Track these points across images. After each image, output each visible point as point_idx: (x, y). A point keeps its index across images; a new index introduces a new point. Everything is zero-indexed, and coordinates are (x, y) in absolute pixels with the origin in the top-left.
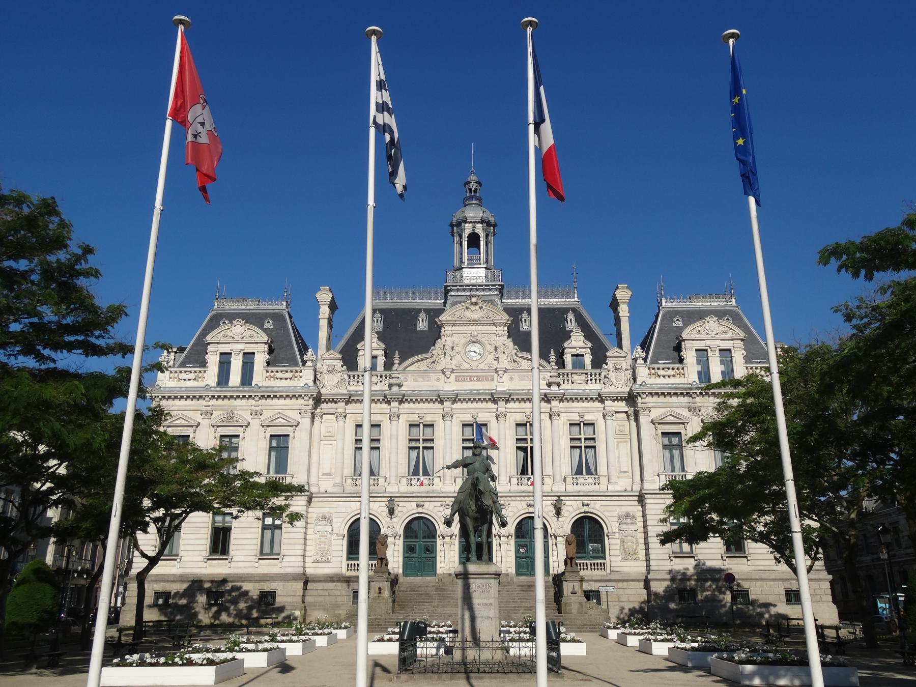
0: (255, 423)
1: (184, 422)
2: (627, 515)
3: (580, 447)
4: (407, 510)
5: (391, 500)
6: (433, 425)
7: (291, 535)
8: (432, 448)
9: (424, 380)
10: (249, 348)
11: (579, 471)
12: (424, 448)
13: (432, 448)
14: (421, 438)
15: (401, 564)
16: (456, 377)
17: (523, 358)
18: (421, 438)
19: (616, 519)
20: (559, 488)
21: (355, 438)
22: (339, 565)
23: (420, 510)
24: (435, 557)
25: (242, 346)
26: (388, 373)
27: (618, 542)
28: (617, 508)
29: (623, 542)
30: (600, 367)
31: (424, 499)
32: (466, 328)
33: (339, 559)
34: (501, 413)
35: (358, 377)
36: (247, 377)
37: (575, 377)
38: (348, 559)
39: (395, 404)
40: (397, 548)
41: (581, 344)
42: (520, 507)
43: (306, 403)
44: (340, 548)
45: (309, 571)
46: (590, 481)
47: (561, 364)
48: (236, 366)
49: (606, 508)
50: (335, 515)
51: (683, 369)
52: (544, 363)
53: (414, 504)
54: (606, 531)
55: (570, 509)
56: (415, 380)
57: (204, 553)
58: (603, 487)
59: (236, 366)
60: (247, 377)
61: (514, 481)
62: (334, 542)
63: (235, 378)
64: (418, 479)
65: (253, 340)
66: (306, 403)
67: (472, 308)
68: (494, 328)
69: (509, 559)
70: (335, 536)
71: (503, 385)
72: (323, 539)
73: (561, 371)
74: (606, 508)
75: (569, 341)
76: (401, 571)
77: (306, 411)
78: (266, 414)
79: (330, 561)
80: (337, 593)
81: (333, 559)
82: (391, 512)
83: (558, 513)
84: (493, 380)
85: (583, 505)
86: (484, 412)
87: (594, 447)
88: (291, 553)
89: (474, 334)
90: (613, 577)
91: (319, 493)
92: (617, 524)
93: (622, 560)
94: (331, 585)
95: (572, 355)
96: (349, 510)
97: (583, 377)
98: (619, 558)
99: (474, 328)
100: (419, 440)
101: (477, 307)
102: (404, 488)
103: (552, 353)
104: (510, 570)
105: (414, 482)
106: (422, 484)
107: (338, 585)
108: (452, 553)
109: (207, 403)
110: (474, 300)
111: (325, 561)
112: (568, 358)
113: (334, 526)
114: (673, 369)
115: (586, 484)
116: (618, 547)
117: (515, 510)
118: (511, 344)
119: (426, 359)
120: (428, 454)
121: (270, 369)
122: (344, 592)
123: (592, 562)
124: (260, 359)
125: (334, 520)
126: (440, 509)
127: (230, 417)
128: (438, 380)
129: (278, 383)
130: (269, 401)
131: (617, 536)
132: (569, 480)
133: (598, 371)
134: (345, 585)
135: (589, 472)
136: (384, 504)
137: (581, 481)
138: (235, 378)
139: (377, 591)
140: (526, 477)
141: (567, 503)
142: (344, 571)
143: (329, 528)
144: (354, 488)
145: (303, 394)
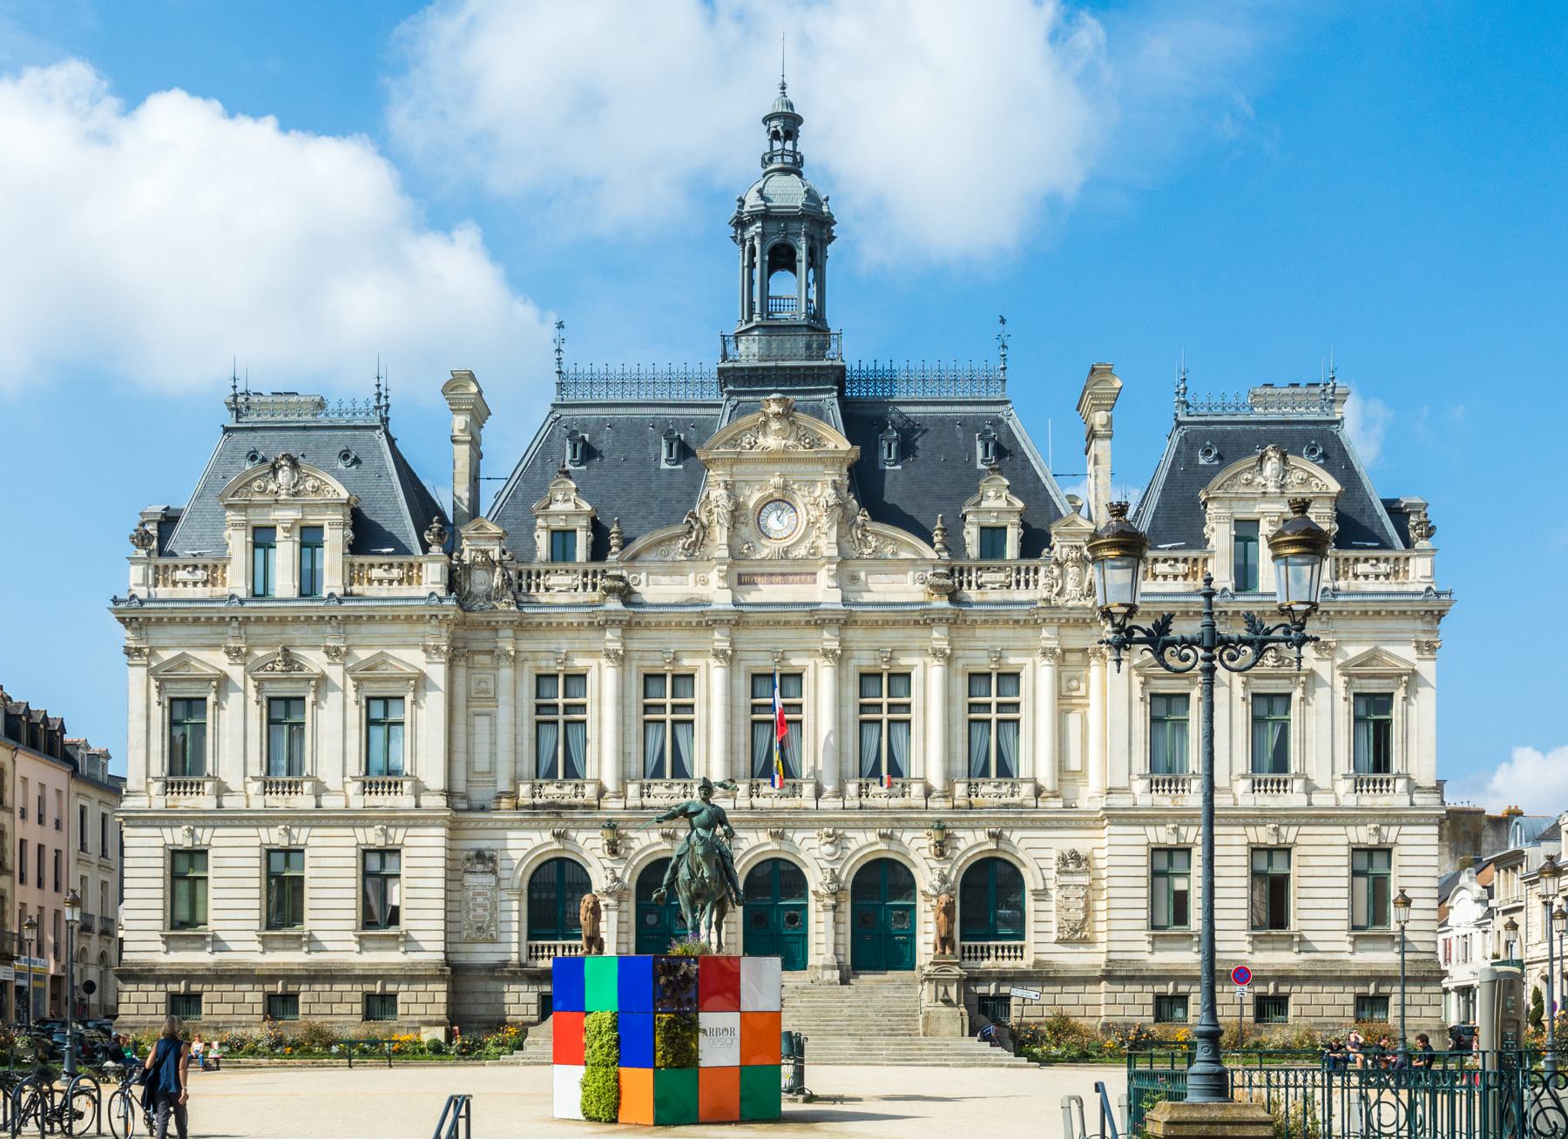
2: (1076, 857)
10: (313, 519)
16: (740, 575)
18: (668, 701)
21: (534, 701)
27: (1053, 906)
30: (1038, 555)
35: (538, 576)
38: (531, 937)
40: (624, 917)
49: (1031, 843)
51: (1206, 560)
57: (256, 925)
72: (480, 900)
74: (1031, 843)
77: (437, 648)
91: (470, 810)
93: (1059, 941)
95: (983, 529)
98: (1054, 937)
111: (486, 941)
112: (971, 536)
114: (1185, 560)
116: (1053, 916)
119: (678, 537)
121: (359, 560)
123: (1000, 943)
124: (334, 540)
128: (705, 583)
130: (365, 629)
143: (489, 880)
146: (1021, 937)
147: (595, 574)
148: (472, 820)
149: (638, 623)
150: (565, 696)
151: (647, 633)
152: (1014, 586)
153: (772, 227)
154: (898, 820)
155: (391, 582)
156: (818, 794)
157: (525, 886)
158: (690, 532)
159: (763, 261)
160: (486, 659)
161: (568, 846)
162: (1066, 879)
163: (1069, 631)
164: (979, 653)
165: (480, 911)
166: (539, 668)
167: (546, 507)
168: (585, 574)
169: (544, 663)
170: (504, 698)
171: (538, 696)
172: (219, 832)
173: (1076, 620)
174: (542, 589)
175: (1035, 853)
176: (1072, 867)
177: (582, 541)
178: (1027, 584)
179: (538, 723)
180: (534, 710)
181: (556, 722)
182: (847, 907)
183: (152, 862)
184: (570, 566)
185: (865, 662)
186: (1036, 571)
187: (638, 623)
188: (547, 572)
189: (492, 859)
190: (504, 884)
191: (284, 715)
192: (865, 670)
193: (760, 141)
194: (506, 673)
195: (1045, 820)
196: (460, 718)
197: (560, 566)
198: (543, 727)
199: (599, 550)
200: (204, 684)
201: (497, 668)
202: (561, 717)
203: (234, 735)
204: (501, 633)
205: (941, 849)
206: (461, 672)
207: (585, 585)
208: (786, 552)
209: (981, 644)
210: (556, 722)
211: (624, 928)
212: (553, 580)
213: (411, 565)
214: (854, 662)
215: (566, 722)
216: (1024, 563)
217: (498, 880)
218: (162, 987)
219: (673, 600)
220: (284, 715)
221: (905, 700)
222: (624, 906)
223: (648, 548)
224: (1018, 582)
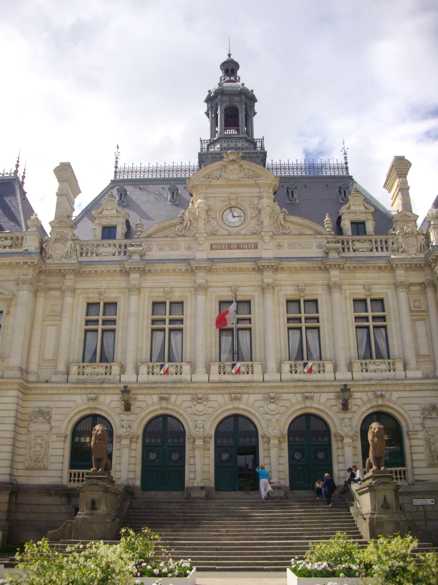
3: (368, 327)
4: (148, 406)
5: (126, 391)
6: (182, 303)
8: (181, 330)
9: (172, 249)
11: (368, 355)
12: (171, 330)
13: (181, 330)
14: (167, 317)
15: (139, 473)
16: (211, 245)
17: (292, 223)
19: (418, 414)
20: (343, 375)
22: (59, 474)
23: (164, 404)
24: (184, 466)
26: (128, 242)
27: (421, 442)
28: (419, 400)
31: (169, 391)
32: (223, 190)
33: (59, 466)
34: (268, 285)
37: (358, 245)
38: (72, 466)
39: (134, 276)
41: (362, 208)
42: (294, 400)
44: (61, 452)
45: (22, 481)
46: (383, 367)
47: (339, 230)
49: (405, 401)
50: (54, 412)
52: (319, 228)
53: (156, 398)
54: (404, 429)
55: (359, 402)
56: (161, 249)
58: (400, 373)
61: (286, 367)
62: (52, 445)
64: (162, 366)
66: (25, 272)
67: (231, 167)
68: (257, 190)
69: (281, 468)
70: (54, 438)
71: (268, 251)
72: (39, 441)
73: (340, 237)
75: (347, 205)
76: (138, 483)
79: (46, 469)
81: (53, 466)
82: (127, 408)
83: (345, 407)
84: (256, 248)
85: (377, 397)
86: (246, 285)
87: (385, 327)
89: (232, 196)
90: (418, 488)
91: (38, 382)
92: (418, 421)
94: (48, 500)
95: (352, 223)
96: (72, 404)
97: (367, 245)
99: (233, 190)
100: (164, 321)
101: (236, 166)
102: (143, 377)
103: (327, 218)
104: (282, 482)
105: (157, 370)
106: (167, 372)
107: (57, 500)
108: (206, 461)
110: (231, 157)
111: (39, 469)
112: (346, 225)
113: (54, 423)
115: (377, 369)
116: (422, 449)
117: (288, 404)
118: (278, 208)
119: (175, 225)
120: (176, 338)
125: (54, 417)
126: (189, 404)
131: (421, 435)
132: (357, 366)
133: (384, 238)
134: (64, 500)
135: (379, 356)
136: (117, 397)
137: (372, 367)
139: (89, 505)
140: (302, 362)
141: (356, 395)
142: (65, 481)
143: (46, 427)
144: (81, 377)
146: (403, 464)
147: (126, 247)
148: (38, 388)
149: (150, 271)
150: (104, 314)
151: (155, 277)
152: (375, 250)
153: (226, 98)
154: (318, 387)
155: (5, 247)
156: (264, 371)
157: (69, 432)
158: (182, 223)
159: (221, 112)
160: (56, 293)
161: (99, 406)
162: (429, 423)
163: (410, 273)
164: (359, 287)
165: (38, 448)
166: (88, 298)
167: (101, 213)
168: (120, 247)
169: (91, 295)
170: (66, 315)
171: (87, 315)
173: (416, 265)
174: (94, 255)
175: (407, 407)
177: (121, 230)
178: (382, 250)
179: (86, 331)
180: (84, 323)
181: (96, 331)
182: (285, 446)
184: (111, 241)
185: (289, 293)
186: (386, 242)
187: (150, 271)
188: (98, 246)
189: (48, 413)
190: (55, 430)
192: (290, 298)
193: (220, 73)
194: (69, 300)
195: (411, 385)
196: (38, 326)
197: (106, 242)
198: (89, 334)
199: (128, 235)
201: (63, 298)
202: (100, 327)
204: (67, 277)
205: (345, 407)
206: (41, 300)
207: (120, 253)
208: (238, 232)
209: (359, 281)
210: (96, 331)
211: (133, 460)
212: (101, 250)
213: (18, 238)
214: (282, 293)
215: (103, 331)
216: (379, 238)
217: (51, 428)
219: (172, 258)
221: (315, 315)
222: (134, 446)
223: (156, 232)
224: (377, 248)
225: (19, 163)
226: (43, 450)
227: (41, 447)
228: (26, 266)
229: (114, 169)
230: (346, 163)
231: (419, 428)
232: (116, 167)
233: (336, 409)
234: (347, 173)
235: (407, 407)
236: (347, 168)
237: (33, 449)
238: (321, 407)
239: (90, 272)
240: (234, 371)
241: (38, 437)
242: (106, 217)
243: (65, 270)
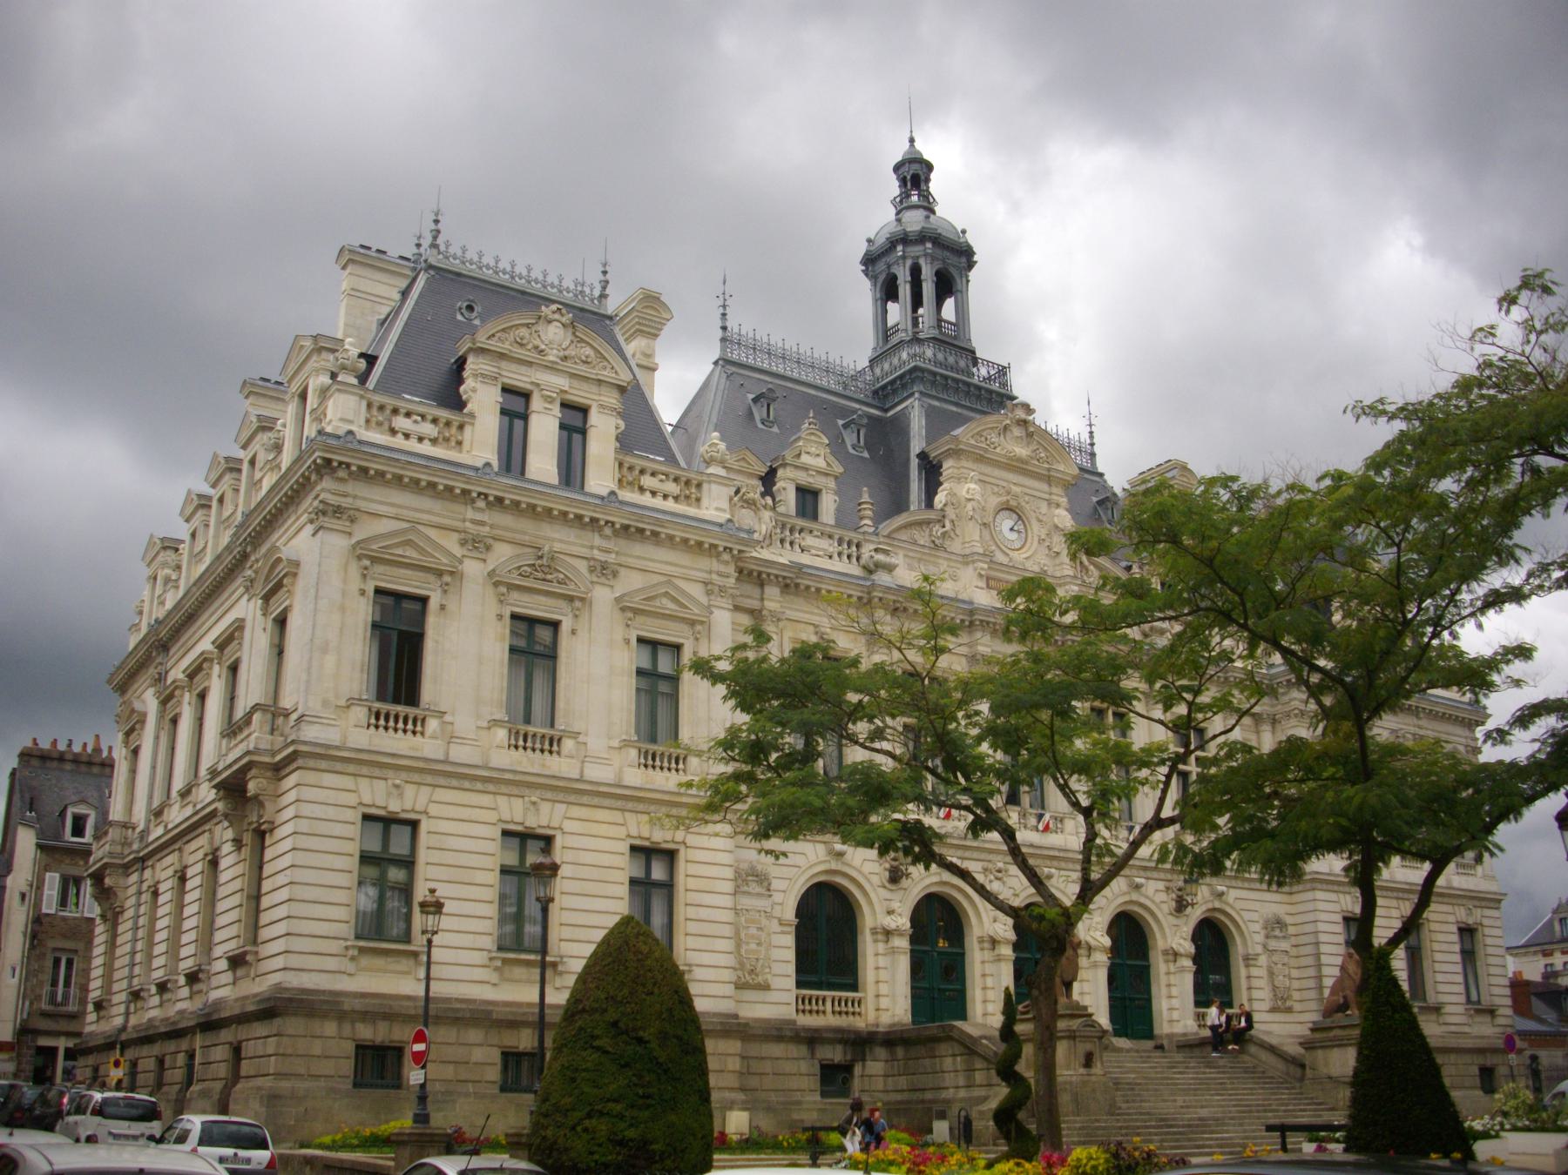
0: (603, 596)
1: (414, 554)
7: (704, 913)
10: (580, 394)
19: (1257, 927)
25: (561, 382)
28: (1257, 906)
29: (1271, 974)
32: (997, 472)
36: (571, 467)
38: (800, 984)
43: (722, 568)
48: (544, 429)
59: (544, 429)
60: (571, 467)
63: (543, 463)
65: (592, 372)
68: (1045, 487)
72: (753, 931)
78: (630, 582)
79: (766, 987)
80: (789, 1067)
81: (776, 983)
88: (706, 958)
94: (776, 1050)
98: (1266, 1006)
109: (479, 516)
122: (804, 1067)
127: (543, 567)
129: (646, 499)
130: (639, 549)
131: (1263, 960)
134: (803, 1050)
138: (543, 463)
139: (1082, 1060)
145: (721, 544)
162: (1273, 944)
165: (753, 946)
172: (442, 795)
175: (1246, 915)
176: (1277, 932)
183: (338, 830)
191: (534, 647)
200: (432, 578)
203: (465, 654)
218: (347, 1030)
220: (534, 647)
225: (608, 276)
226: (762, 948)
227: (759, 944)
228: (726, 557)
229: (720, 333)
230: (1092, 445)
231: (1259, 949)
232: (724, 328)
233: (1165, 908)
234: (1093, 463)
235: (1246, 915)
236: (1093, 455)
237: (744, 947)
238: (1148, 903)
239: (808, 587)
240: (1041, 827)
241: (753, 922)
242: (805, 468)
243: (769, 575)
